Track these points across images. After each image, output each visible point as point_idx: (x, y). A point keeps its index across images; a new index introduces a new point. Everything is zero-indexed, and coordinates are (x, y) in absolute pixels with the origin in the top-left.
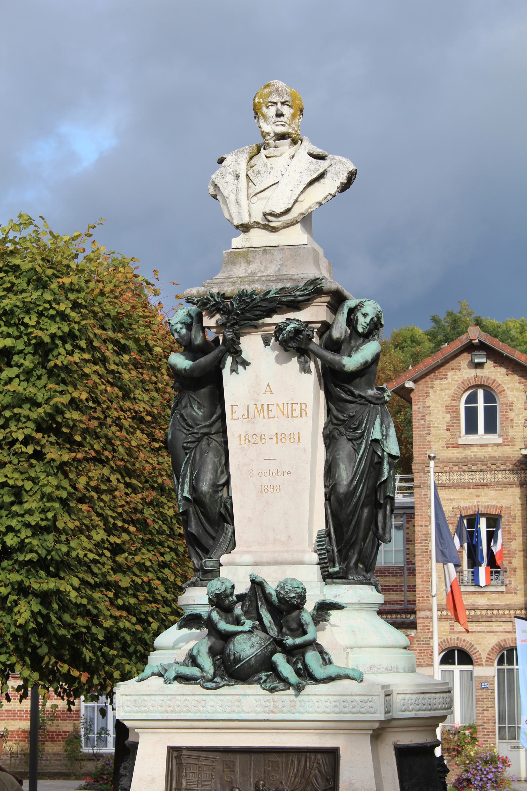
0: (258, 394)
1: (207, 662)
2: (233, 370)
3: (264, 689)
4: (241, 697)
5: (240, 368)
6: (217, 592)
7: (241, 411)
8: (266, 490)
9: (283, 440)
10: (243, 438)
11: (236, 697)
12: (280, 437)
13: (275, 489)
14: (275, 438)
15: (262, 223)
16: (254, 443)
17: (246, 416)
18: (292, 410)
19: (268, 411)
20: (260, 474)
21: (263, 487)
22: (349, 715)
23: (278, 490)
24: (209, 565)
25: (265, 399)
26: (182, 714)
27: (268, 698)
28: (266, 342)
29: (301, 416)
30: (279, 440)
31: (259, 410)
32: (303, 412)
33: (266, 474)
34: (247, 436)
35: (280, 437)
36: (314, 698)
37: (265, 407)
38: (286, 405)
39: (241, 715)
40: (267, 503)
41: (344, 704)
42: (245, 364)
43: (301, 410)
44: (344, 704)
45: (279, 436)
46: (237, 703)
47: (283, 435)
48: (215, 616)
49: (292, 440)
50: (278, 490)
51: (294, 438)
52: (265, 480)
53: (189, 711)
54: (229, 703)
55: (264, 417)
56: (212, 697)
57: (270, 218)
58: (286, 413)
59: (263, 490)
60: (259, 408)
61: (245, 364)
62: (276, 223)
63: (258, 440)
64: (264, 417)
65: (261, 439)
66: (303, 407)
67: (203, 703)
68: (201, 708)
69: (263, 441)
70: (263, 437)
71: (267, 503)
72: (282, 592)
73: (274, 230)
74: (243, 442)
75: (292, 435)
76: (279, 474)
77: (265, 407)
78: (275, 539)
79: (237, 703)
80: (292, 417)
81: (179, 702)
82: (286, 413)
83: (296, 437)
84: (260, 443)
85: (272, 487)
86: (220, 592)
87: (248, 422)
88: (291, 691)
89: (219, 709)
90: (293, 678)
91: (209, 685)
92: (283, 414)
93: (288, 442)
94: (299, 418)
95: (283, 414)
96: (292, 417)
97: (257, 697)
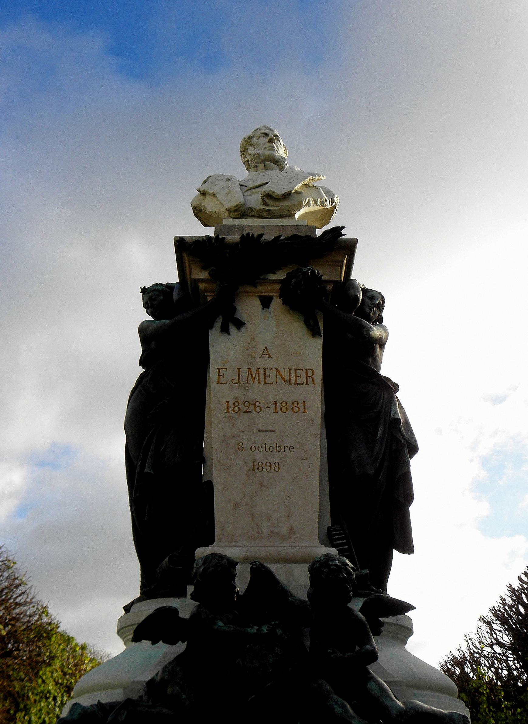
0: (253, 357)
2: (225, 330)
5: (232, 329)
7: (229, 375)
8: (260, 468)
9: (284, 409)
10: (231, 405)
12: (280, 407)
13: (273, 466)
14: (273, 407)
15: (257, 208)
16: (246, 412)
17: (236, 381)
18: (296, 376)
19: (265, 376)
20: (253, 448)
21: (256, 463)
23: (277, 469)
25: (261, 363)
28: (266, 302)
29: (307, 384)
30: (278, 409)
31: (254, 375)
32: (310, 380)
33: (260, 449)
34: (236, 404)
35: (280, 407)
37: (262, 372)
38: (287, 370)
40: (261, 484)
42: (240, 324)
43: (307, 376)
45: (279, 405)
47: (284, 404)
49: (296, 409)
50: (277, 469)
51: (298, 407)
52: (259, 456)
55: (259, 383)
57: (268, 201)
58: (287, 379)
59: (256, 467)
60: (254, 373)
61: (240, 324)
62: (273, 207)
63: (251, 408)
64: (259, 383)
65: (255, 407)
66: (310, 373)
69: (258, 410)
70: (257, 405)
71: (261, 484)
73: (271, 215)
74: (231, 409)
75: (295, 404)
76: (278, 448)
77: (262, 372)
78: (271, 532)
80: (296, 383)
82: (287, 379)
83: (301, 406)
84: (253, 411)
85: (268, 465)
87: (239, 387)
92: (284, 380)
93: (290, 412)
94: (304, 385)
95: (284, 380)
96: (296, 383)
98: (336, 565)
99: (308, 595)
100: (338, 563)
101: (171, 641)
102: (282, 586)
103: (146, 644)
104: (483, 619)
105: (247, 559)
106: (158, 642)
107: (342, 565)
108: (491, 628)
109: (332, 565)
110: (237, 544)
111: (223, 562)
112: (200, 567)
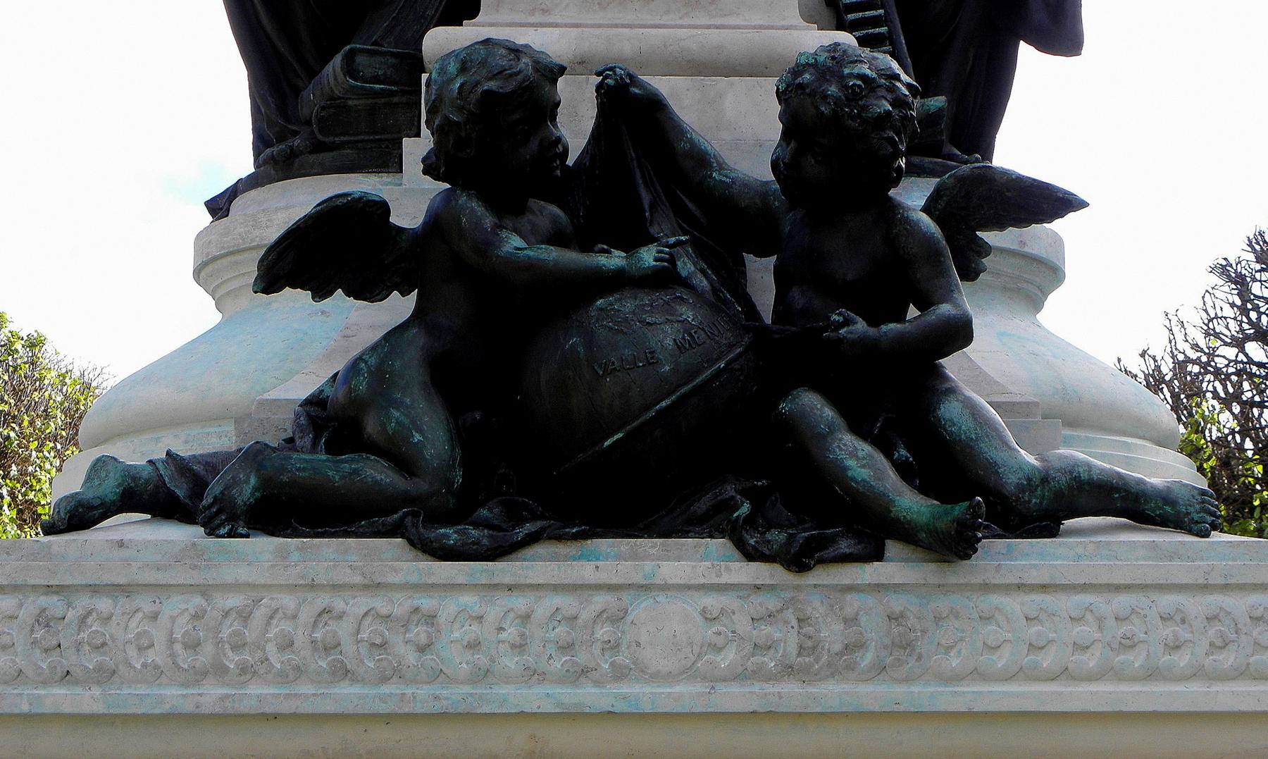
1: (429, 431)
3: (751, 555)
4: (626, 597)
6: (492, 85)
11: (601, 600)
22: (1195, 687)
24: (368, 72)
26: (306, 689)
27: (772, 603)
36: (1014, 605)
39: (625, 689)
41: (1168, 631)
44: (1168, 631)
46: (603, 632)
48: (473, 209)
53: (342, 672)
54: (561, 630)
56: (469, 600)
67: (419, 632)
68: (411, 657)
72: (833, 89)
79: (603, 632)
81: (286, 626)
86: (509, 88)
88: (896, 568)
89: (511, 663)
90: (910, 503)
91: (450, 534)
97: (713, 602)
98: (863, 77)
99: (775, 166)
100: (868, 72)
101: (367, 290)
102: (691, 141)
103: (295, 299)
104: (1223, 270)
105: (581, 63)
106: (330, 293)
107: (880, 76)
108: (1244, 293)
109: (851, 75)
110: (551, 19)
111: (522, 65)
112: (452, 80)
